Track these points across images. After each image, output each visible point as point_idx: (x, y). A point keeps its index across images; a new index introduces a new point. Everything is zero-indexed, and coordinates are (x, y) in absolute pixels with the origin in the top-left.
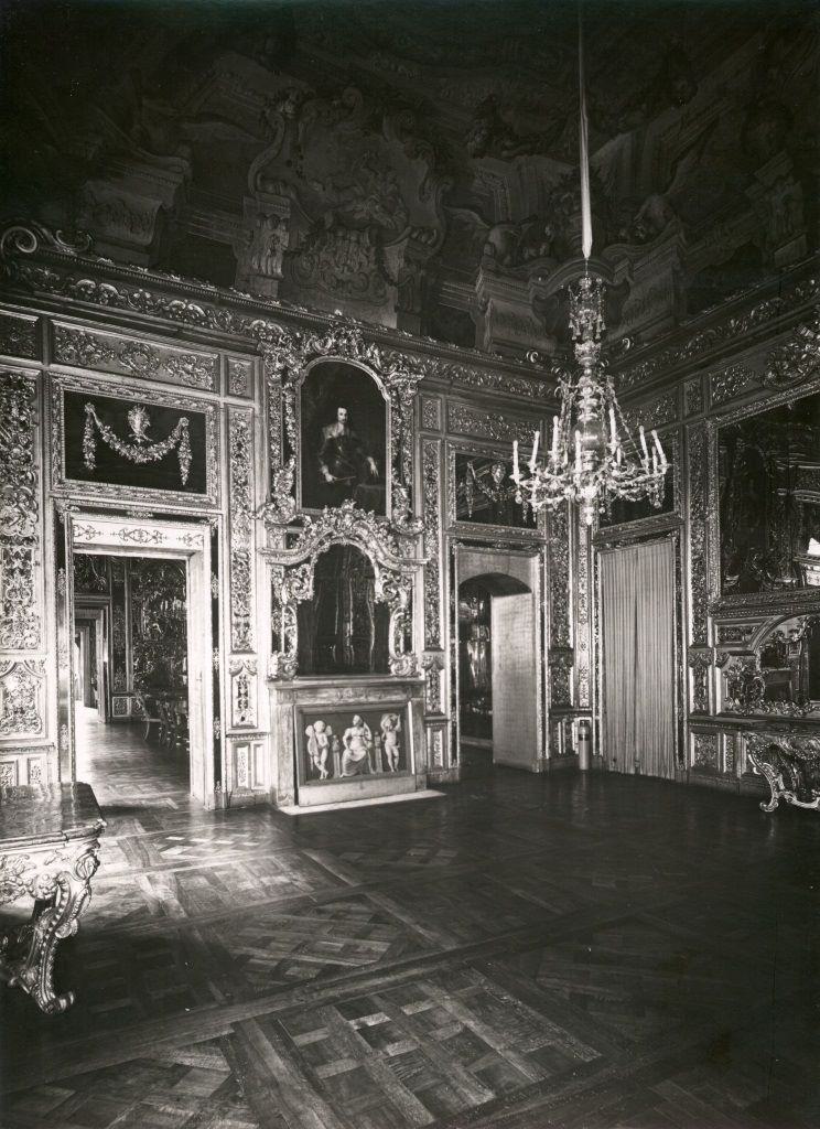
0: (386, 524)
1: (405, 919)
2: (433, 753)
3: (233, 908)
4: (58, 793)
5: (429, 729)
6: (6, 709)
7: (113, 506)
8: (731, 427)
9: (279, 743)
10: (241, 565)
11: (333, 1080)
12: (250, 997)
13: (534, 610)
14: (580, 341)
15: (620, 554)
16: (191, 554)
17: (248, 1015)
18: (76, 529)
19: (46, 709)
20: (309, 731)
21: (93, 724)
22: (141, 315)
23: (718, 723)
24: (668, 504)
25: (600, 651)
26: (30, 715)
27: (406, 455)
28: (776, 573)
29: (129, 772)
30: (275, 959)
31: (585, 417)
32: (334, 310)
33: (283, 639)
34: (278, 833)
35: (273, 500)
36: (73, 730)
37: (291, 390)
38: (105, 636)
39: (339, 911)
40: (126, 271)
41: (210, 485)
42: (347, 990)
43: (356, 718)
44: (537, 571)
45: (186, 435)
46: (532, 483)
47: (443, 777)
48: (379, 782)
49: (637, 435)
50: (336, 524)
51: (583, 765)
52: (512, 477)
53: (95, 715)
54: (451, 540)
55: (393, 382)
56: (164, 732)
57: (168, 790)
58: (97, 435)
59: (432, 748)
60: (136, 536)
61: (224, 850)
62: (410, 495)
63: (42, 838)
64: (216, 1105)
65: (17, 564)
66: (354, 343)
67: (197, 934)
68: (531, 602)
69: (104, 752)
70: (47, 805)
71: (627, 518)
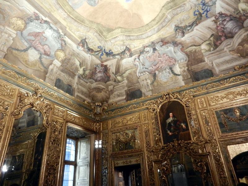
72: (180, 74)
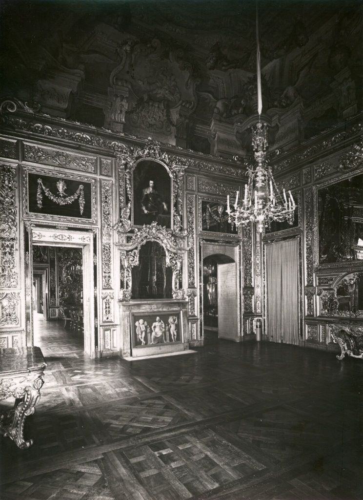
0: (171, 232)
23: (318, 320)
27: (180, 201)
37: (129, 173)
50: (149, 232)
54: (200, 239)
62: (181, 219)
72: (175, 124)
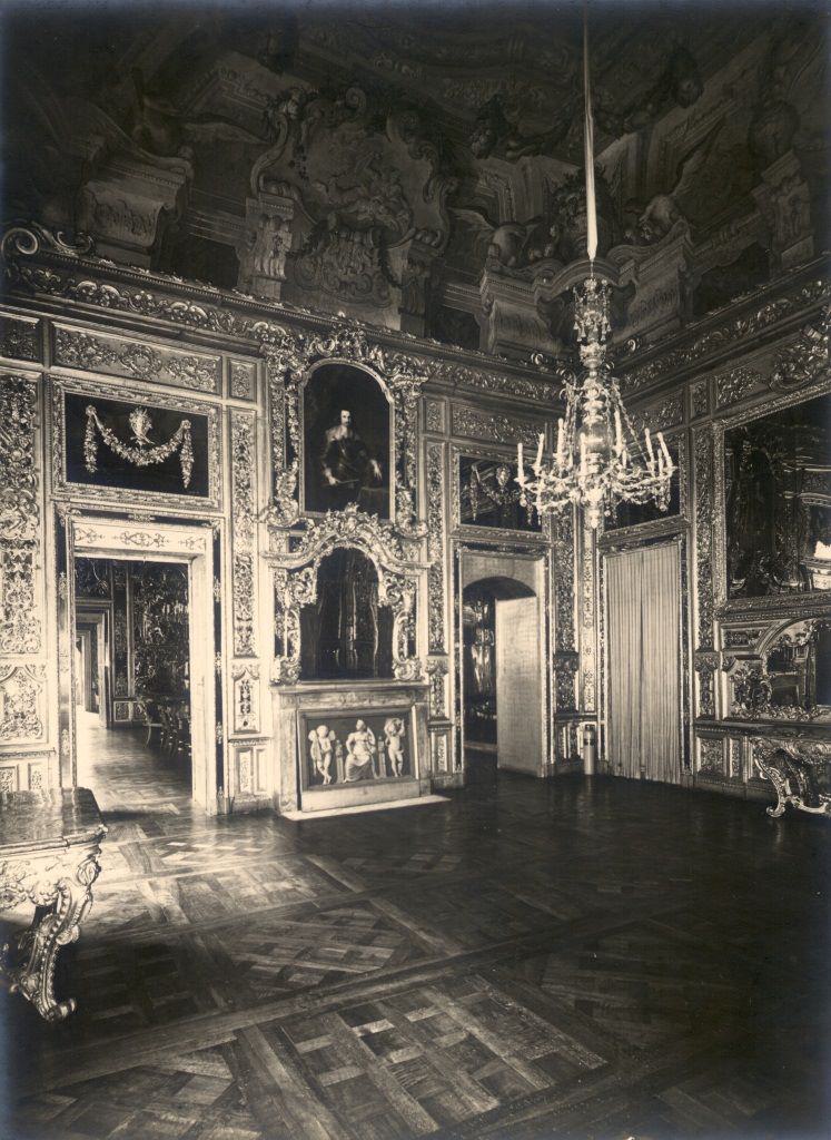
0: (390, 527)
1: (408, 925)
2: (437, 758)
3: (236, 914)
4: (59, 799)
5: (433, 734)
6: (6, 713)
7: (114, 510)
8: (737, 430)
9: (281, 748)
10: (243, 568)
11: (337, 1087)
12: (253, 1004)
13: (539, 614)
14: (585, 343)
15: (626, 560)
16: (193, 558)
17: (251, 1022)
18: (77, 532)
19: (47, 712)
20: (312, 736)
21: (94, 729)
22: (142, 317)
23: (725, 727)
24: (674, 507)
25: (606, 655)
26: (30, 720)
27: (409, 458)
28: (783, 576)
29: (129, 777)
30: (279, 966)
31: (590, 420)
32: (338, 310)
33: (286, 642)
34: (281, 838)
35: (276, 503)
36: (74, 735)
37: (295, 392)
38: (106, 641)
39: (342, 917)
40: (128, 273)
41: (212, 488)
42: (351, 997)
43: (360, 723)
44: (542, 575)
45: (188, 438)
46: (536, 485)
47: (447, 782)
48: (383, 787)
49: (642, 437)
50: (340, 527)
51: (589, 770)
52: (516, 480)
53: (98, 720)
54: (455, 543)
55: (397, 384)
56: (165, 737)
57: (169, 796)
58: (98, 438)
59: (436, 753)
60: (138, 539)
61: (227, 856)
62: (413, 498)
63: (43, 844)
64: (218, 1113)
65: (18, 567)
66: (357, 345)
67: (199, 941)
68: (536, 606)
69: (105, 757)
70: (48, 811)
71: (634, 520)
